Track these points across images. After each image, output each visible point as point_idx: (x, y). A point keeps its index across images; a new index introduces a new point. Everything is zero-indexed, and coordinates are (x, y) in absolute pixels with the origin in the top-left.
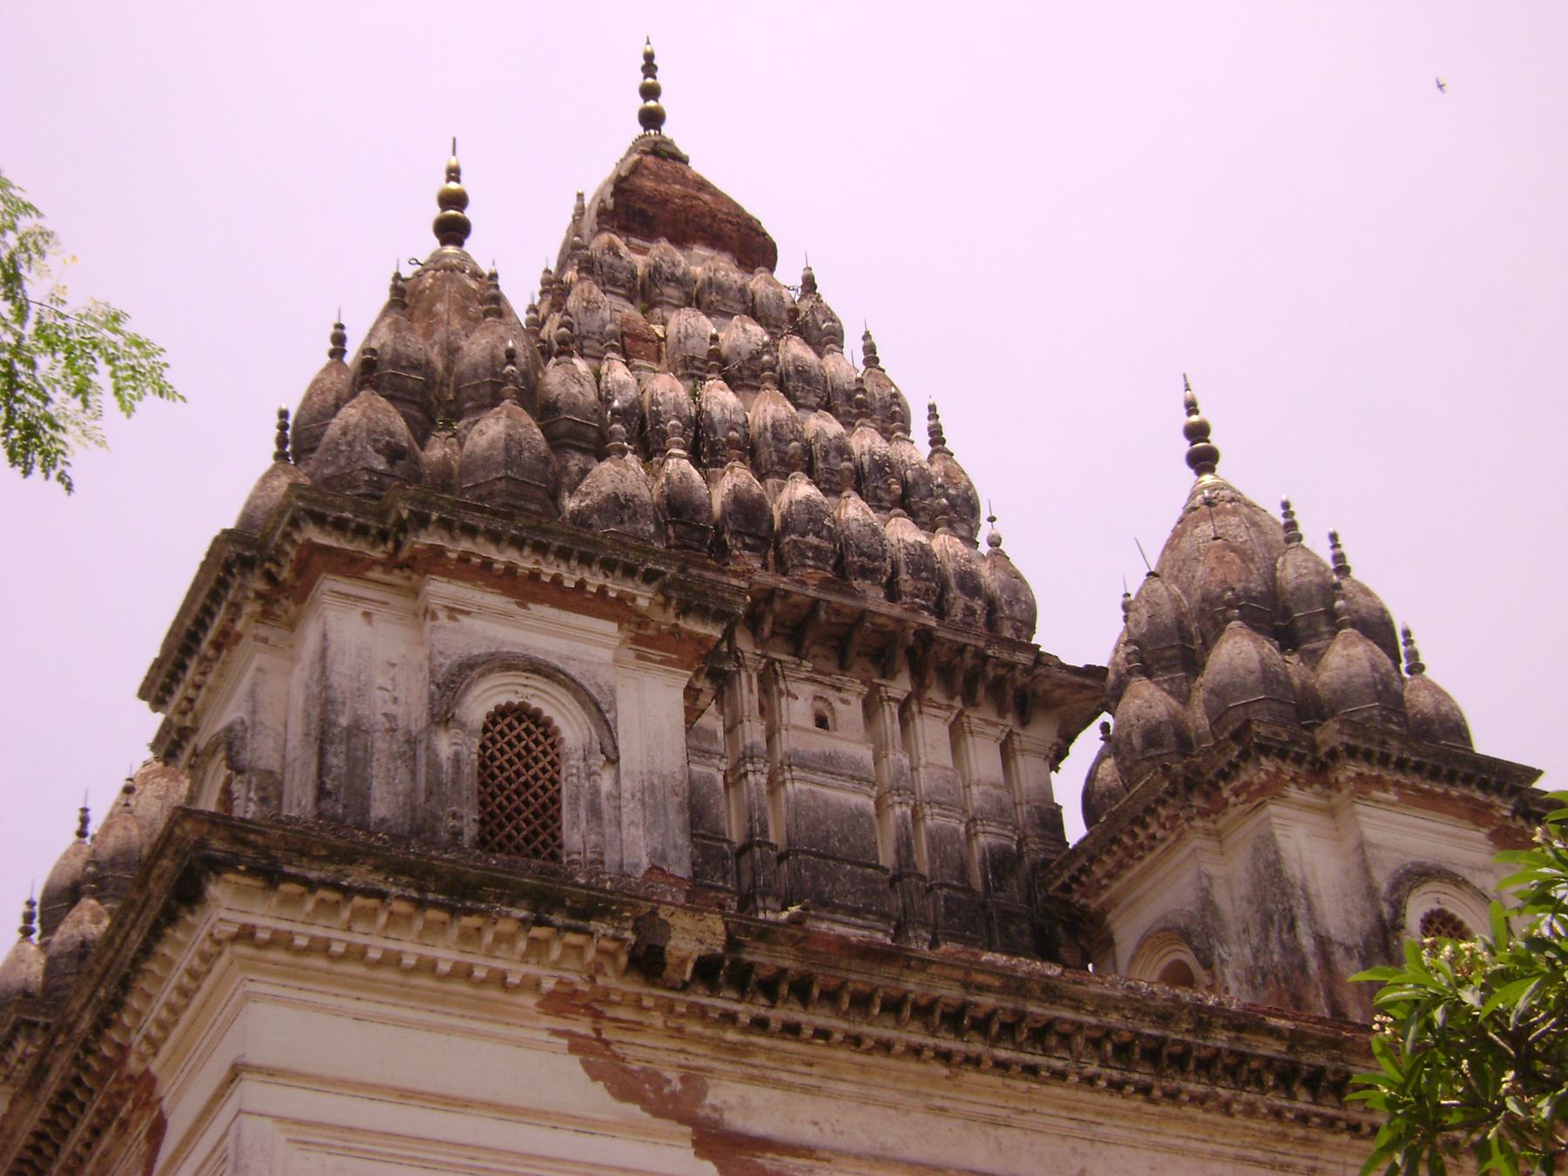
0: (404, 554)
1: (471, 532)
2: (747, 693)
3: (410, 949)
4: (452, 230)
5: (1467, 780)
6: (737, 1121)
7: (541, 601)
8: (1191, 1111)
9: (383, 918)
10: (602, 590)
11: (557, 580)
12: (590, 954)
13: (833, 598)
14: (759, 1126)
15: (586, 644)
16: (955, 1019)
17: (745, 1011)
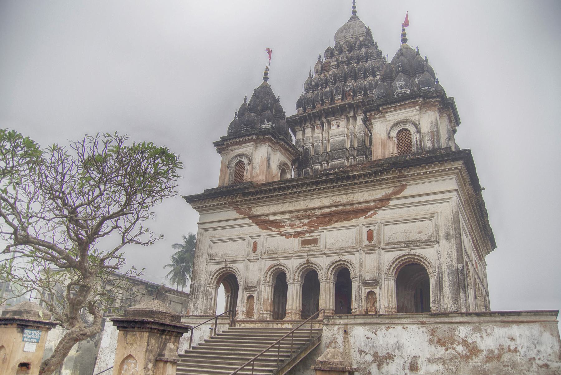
1: (230, 139)
2: (326, 128)
3: (211, 204)
4: (266, 79)
5: (408, 99)
6: (255, 213)
8: (325, 190)
14: (258, 213)
16: (279, 189)
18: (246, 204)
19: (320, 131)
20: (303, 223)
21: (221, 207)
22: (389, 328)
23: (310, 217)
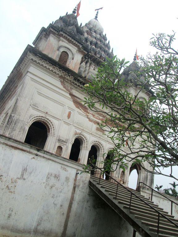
0: (59, 34)
1: (66, 34)
2: (88, 65)
3: (48, 67)
6: (74, 94)
7: (71, 43)
9: (46, 63)
10: (77, 44)
11: (73, 42)
12: (65, 74)
13: (99, 59)
14: (76, 95)
15: (74, 49)
17: (78, 84)
18: (71, 84)
19: (85, 64)
20: (99, 118)
21: (54, 74)
22: (163, 201)
23: (104, 117)
